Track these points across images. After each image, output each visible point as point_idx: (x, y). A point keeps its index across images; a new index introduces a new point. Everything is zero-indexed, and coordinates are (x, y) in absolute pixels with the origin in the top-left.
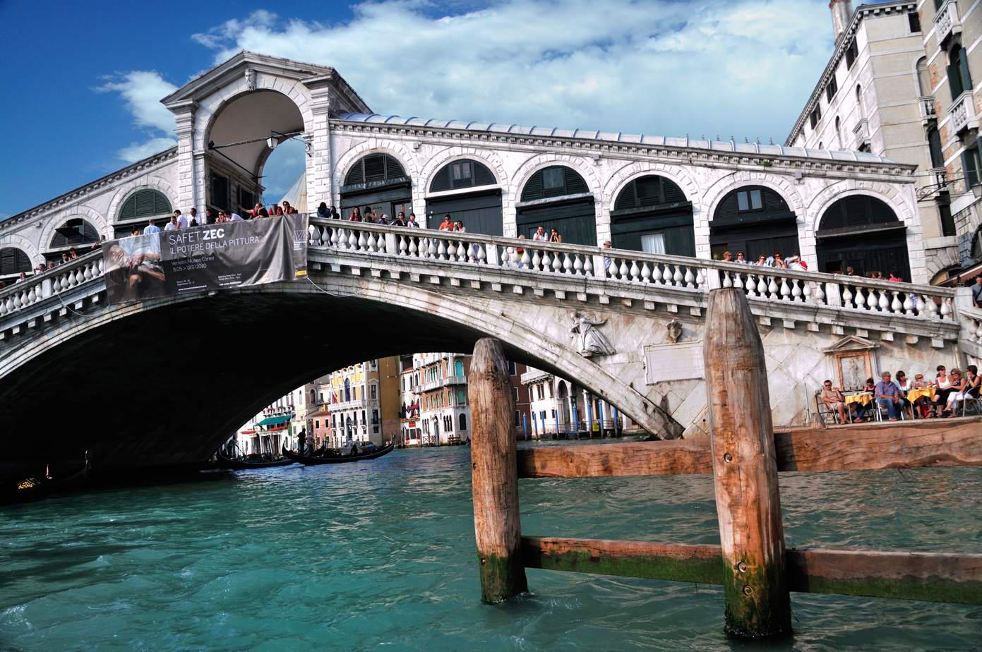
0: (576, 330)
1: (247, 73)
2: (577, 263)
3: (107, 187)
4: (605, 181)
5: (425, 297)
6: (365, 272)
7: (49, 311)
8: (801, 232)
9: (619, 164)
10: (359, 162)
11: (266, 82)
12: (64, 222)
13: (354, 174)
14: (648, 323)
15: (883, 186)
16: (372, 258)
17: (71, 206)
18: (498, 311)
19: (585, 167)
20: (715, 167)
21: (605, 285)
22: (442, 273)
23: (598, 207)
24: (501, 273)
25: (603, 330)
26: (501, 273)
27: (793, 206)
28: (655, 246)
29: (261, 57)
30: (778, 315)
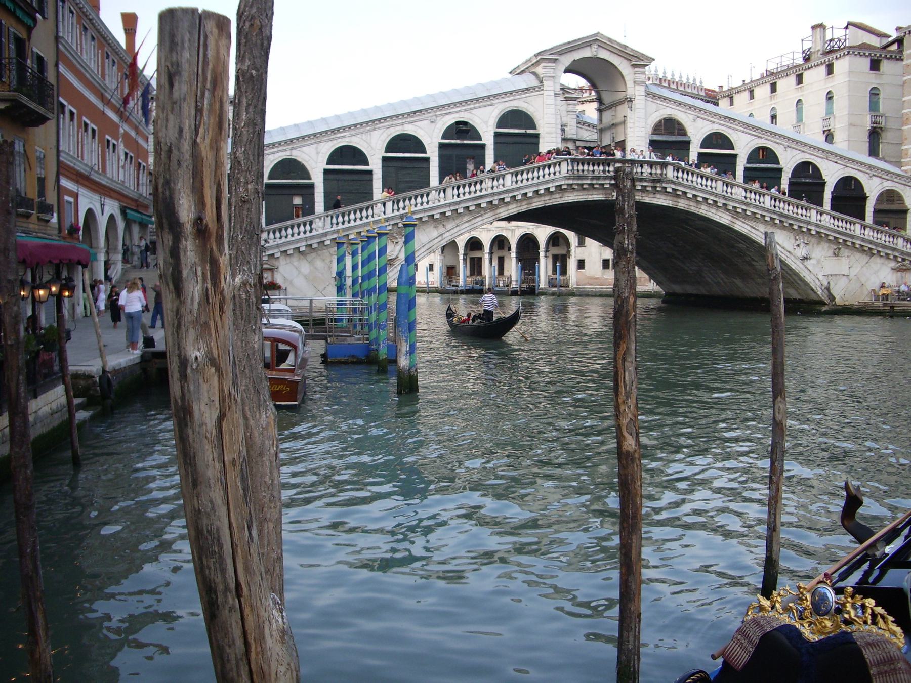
0: (798, 246)
3: (489, 103)
4: (788, 161)
5: (730, 218)
6: (706, 199)
7: (511, 195)
8: (868, 202)
9: (795, 152)
10: (660, 122)
11: (604, 54)
12: (453, 122)
14: (826, 245)
15: (902, 187)
16: (712, 194)
17: (459, 111)
22: (744, 207)
23: (783, 173)
24: (774, 212)
26: (774, 212)
27: (866, 190)
29: (610, 40)
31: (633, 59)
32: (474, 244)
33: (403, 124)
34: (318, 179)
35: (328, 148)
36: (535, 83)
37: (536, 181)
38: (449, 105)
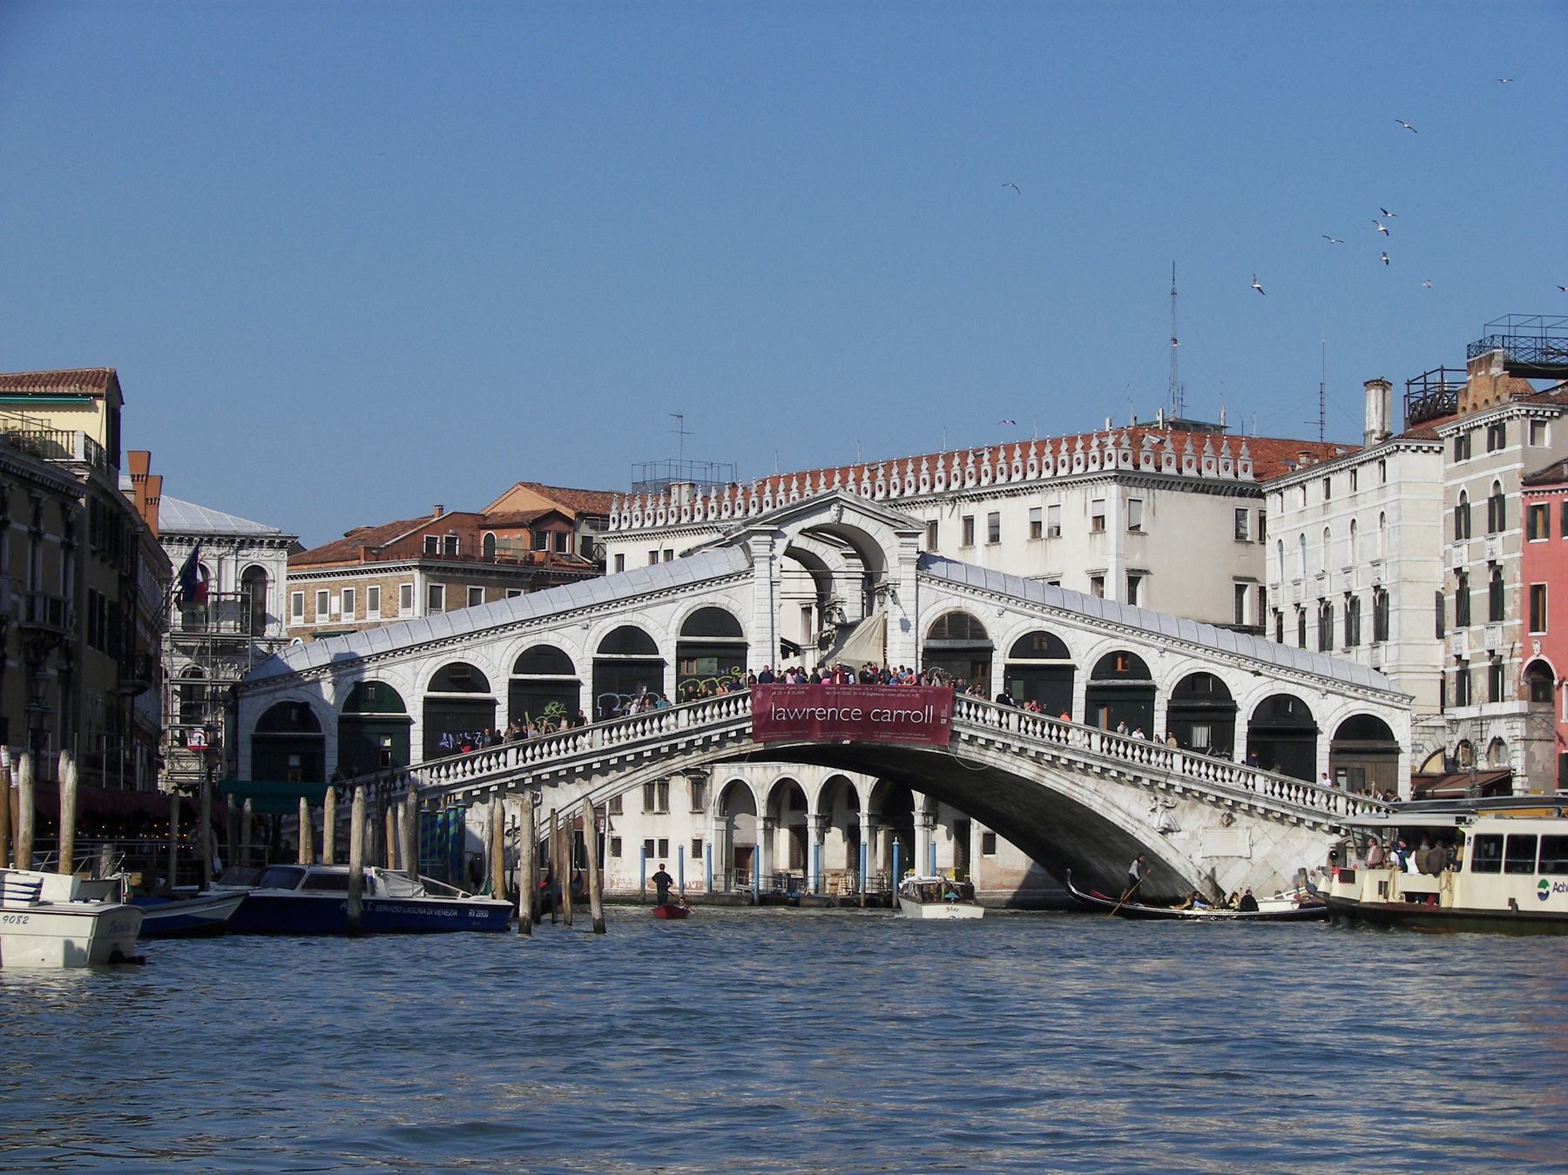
0: (1154, 810)
1: (835, 507)
2: (1161, 758)
3: (670, 597)
4: (1166, 672)
5: (1035, 769)
10: (942, 618)
11: (850, 518)
13: (937, 630)
14: (1209, 808)
16: (999, 733)
18: (1092, 787)
19: (1149, 657)
20: (1257, 673)
21: (1183, 779)
25: (1172, 812)
26: (1105, 759)
28: (1201, 735)
30: (1302, 816)
31: (898, 525)
32: (787, 797)
33: (540, 632)
34: (415, 710)
35: (430, 665)
36: (744, 566)
37: (724, 718)
38: (609, 603)
